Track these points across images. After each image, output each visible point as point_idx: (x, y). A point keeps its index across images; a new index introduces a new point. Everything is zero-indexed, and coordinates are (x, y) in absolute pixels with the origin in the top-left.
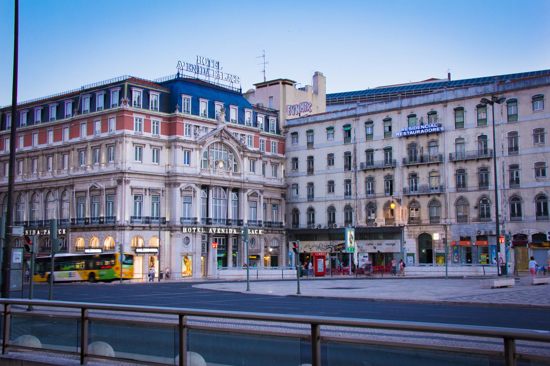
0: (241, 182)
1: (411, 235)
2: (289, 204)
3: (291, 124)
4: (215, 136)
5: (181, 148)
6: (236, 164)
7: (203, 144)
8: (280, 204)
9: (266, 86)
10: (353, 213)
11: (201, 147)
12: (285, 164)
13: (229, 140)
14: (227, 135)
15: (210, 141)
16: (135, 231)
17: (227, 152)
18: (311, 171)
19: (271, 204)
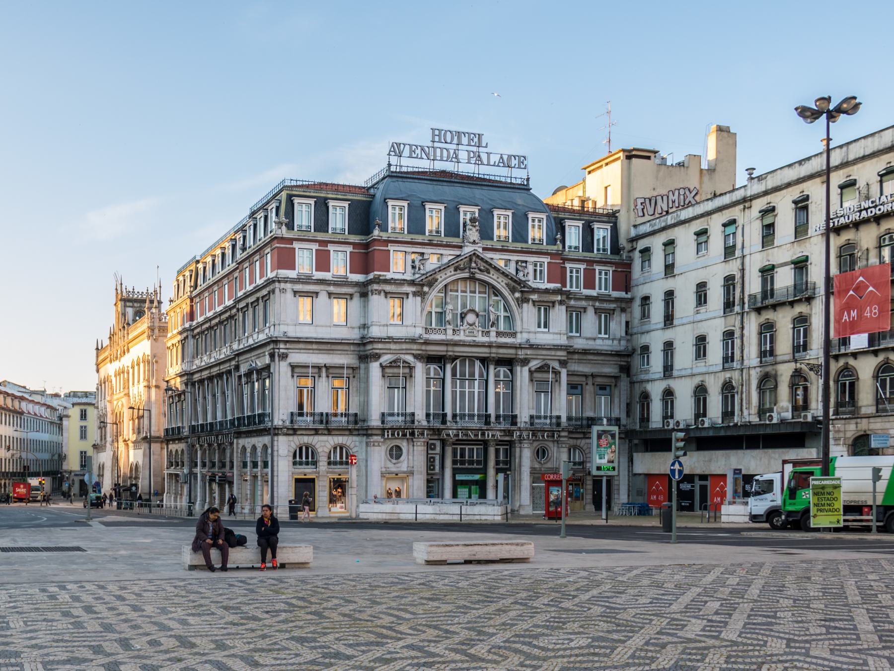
0: (516, 348)
1: (839, 439)
2: (635, 384)
3: (641, 233)
5: (382, 294)
6: (509, 315)
7: (431, 284)
8: (616, 385)
9: (601, 167)
10: (736, 395)
11: (426, 289)
12: (629, 310)
13: (489, 273)
14: (485, 265)
15: (445, 279)
16: (300, 437)
17: (487, 296)
18: (669, 319)
19: (593, 384)
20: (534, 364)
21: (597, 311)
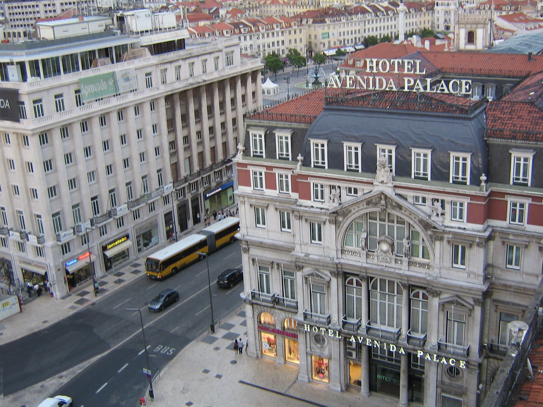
4: (368, 203)
20: (445, 296)
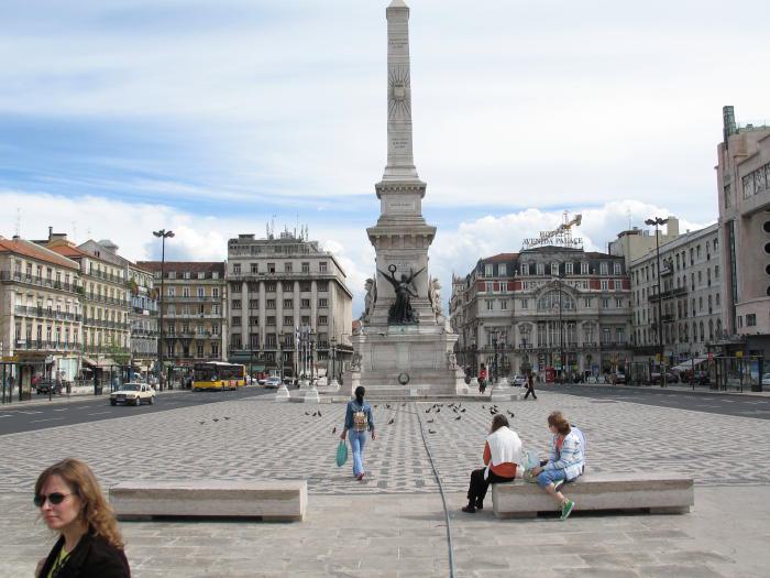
21: (616, 299)
